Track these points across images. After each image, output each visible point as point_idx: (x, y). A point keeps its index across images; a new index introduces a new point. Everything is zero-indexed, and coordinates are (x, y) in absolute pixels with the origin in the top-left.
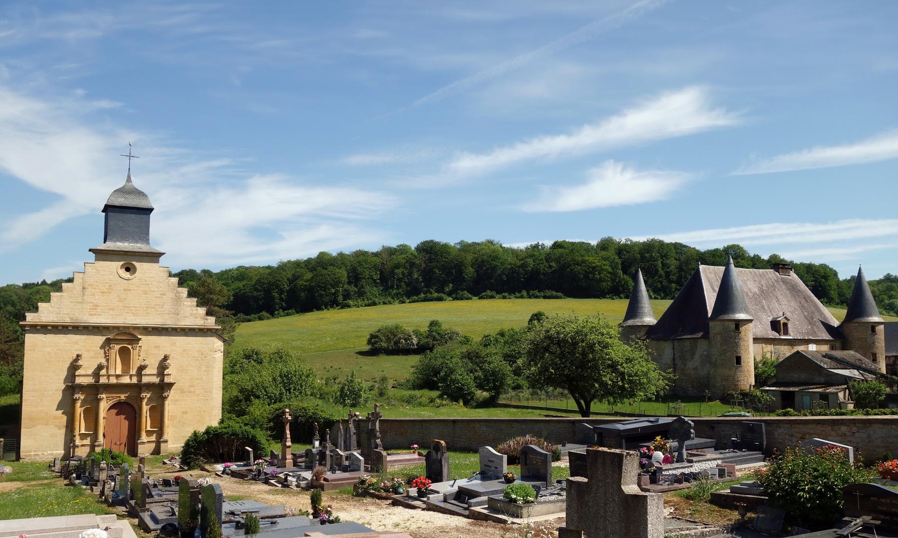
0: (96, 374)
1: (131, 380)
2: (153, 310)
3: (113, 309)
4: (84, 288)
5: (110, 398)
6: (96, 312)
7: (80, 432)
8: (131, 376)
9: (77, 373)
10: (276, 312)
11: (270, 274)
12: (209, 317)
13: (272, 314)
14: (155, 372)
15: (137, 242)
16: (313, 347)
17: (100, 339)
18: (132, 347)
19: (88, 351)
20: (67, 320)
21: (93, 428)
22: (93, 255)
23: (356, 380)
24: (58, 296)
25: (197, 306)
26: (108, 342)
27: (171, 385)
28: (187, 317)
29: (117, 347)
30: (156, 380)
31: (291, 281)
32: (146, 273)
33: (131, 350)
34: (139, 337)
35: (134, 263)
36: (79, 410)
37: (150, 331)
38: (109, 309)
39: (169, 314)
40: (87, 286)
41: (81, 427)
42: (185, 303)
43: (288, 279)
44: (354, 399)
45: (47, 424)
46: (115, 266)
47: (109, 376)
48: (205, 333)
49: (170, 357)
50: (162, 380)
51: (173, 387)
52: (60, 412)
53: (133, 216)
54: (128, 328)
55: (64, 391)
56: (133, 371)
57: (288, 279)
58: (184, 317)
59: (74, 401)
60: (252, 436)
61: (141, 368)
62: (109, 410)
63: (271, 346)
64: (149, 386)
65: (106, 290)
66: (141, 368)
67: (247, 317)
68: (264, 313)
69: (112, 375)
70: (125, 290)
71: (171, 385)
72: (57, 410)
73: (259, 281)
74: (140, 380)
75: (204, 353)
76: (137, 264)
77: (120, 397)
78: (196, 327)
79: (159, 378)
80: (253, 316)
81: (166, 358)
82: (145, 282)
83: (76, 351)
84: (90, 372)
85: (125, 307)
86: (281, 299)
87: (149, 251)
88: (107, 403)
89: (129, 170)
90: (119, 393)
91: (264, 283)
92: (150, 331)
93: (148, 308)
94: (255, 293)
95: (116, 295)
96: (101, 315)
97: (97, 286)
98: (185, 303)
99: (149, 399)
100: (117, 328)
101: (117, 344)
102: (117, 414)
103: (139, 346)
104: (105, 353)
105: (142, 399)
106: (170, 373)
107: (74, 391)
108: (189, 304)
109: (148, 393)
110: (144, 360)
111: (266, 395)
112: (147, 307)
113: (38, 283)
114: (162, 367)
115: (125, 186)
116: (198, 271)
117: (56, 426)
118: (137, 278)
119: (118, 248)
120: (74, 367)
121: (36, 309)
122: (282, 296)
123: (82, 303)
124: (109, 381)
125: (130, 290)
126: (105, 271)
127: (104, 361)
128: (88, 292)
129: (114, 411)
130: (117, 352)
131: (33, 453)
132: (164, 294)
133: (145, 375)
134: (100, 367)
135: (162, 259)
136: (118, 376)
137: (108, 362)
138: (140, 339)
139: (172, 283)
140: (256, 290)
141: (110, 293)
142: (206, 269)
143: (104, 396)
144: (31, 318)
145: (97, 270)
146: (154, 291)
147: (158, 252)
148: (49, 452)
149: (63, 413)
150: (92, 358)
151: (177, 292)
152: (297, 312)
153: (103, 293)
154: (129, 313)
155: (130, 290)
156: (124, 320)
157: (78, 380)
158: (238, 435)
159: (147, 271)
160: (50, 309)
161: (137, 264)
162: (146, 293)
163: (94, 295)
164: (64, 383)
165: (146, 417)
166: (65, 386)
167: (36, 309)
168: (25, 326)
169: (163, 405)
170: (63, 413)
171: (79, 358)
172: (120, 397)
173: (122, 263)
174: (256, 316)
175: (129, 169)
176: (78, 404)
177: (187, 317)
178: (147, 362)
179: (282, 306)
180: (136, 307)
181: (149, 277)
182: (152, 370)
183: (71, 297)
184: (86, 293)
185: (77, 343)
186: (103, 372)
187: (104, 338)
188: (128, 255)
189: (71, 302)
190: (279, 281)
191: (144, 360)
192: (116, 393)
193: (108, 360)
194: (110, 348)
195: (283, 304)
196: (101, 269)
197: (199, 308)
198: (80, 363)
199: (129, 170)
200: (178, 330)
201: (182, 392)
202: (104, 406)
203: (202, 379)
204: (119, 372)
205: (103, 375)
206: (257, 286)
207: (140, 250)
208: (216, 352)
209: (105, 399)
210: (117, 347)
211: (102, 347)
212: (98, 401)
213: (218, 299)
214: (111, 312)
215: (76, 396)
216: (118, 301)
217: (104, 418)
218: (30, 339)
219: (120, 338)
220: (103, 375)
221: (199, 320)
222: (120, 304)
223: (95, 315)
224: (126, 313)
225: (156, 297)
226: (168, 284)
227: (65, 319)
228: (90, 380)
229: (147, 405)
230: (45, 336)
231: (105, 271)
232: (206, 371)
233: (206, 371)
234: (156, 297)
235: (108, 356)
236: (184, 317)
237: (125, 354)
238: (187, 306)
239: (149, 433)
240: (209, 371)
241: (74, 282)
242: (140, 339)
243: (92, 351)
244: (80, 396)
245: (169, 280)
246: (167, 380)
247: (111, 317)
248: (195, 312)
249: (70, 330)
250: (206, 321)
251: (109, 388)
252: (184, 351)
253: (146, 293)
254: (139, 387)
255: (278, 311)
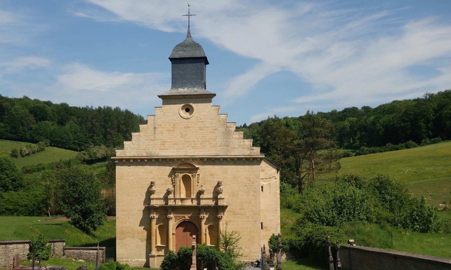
0: (166, 198)
1: (192, 203)
2: (208, 143)
3: (176, 144)
4: (155, 128)
5: (178, 218)
6: (164, 147)
7: (156, 245)
8: (192, 200)
9: (152, 197)
10: (423, 141)
11: (416, 106)
12: (255, 148)
13: (419, 142)
14: (211, 196)
15: (194, 87)
16: (444, 172)
17: (168, 169)
18: (192, 176)
19: (160, 179)
20: (143, 154)
21: (166, 243)
22: (161, 100)
23: (426, 205)
24: (137, 136)
25: (130, 140)
26: (174, 171)
27: (224, 208)
28: (236, 148)
29: (181, 175)
30: (211, 203)
31: (436, 111)
32: (201, 112)
33: (192, 178)
34: (197, 166)
35: (191, 104)
36: (155, 227)
37: (206, 162)
38: (174, 144)
39: (221, 146)
40: (157, 126)
41: (157, 241)
42: (234, 136)
43: (434, 109)
44: (424, 224)
45: (133, 237)
46: (177, 108)
47: (175, 199)
48: (251, 162)
49: (222, 184)
50: (216, 203)
51: (227, 210)
52: (142, 228)
53: (180, 63)
54: (188, 159)
55: (144, 211)
56: (194, 196)
57: (434, 109)
58: (234, 148)
59: (151, 219)
60: (216, 259)
61: (200, 193)
62: (177, 227)
63: (404, 172)
64: (206, 208)
65: (171, 129)
66: (200, 193)
67: (394, 146)
68: (411, 142)
69: (178, 199)
70: (185, 128)
71: (224, 208)
72: (140, 226)
73: (406, 112)
74: (199, 203)
75: (252, 180)
76: (194, 105)
77: (185, 217)
78: (243, 156)
79: (214, 202)
80: (400, 144)
81: (219, 184)
82: (200, 120)
83: (151, 178)
84: (162, 196)
85: (186, 142)
86: (428, 128)
87: (202, 93)
88: (175, 221)
89: (189, 27)
90: (184, 214)
91: (410, 115)
92: (206, 162)
93: (204, 141)
94: (403, 124)
95: (179, 132)
96: (168, 149)
97: (165, 125)
98: (234, 136)
99: (207, 219)
100: (178, 159)
101: (180, 173)
102: (184, 231)
103: (198, 175)
104: (172, 180)
105: (201, 219)
106: (222, 197)
107: (150, 212)
108: (237, 136)
109: (206, 214)
110: (202, 186)
111: (318, 219)
112: (203, 141)
113: (241, 126)
114: (217, 192)
115: (185, 40)
116: (360, 108)
117: (139, 239)
118: (194, 117)
119: (179, 93)
120: (150, 192)
121: (122, 147)
122: (429, 125)
123: (154, 140)
124: (175, 203)
125: (189, 127)
126: (170, 113)
127: (171, 187)
128: (158, 131)
129: (181, 229)
130: (181, 180)
131: (124, 260)
132: (216, 129)
133: (203, 199)
134: (168, 192)
135: (213, 99)
136: (182, 200)
137: (175, 188)
138: (198, 169)
139: (222, 119)
140: (404, 121)
141: (174, 131)
142: (366, 105)
143: (172, 216)
144: (119, 153)
145: (164, 112)
146: (208, 127)
147: (210, 93)
148: (136, 260)
149: (144, 229)
150: (162, 184)
151: (227, 127)
152: (443, 140)
153: (169, 131)
154: (189, 147)
155: (189, 127)
156: (185, 153)
157: (153, 203)
158: (204, 256)
159: (202, 111)
160: (132, 146)
161: (194, 105)
162: (201, 129)
163: (162, 133)
164: (144, 205)
165: (206, 234)
166: (144, 207)
167: (122, 147)
168: (115, 160)
169: (218, 225)
170: (144, 229)
171: (152, 185)
172: (185, 217)
173: (182, 105)
174: (403, 145)
175: (189, 26)
176: (154, 222)
177: (236, 148)
178: (204, 188)
179: (429, 134)
180: (194, 141)
181: (204, 115)
182: (208, 194)
183: (146, 136)
184: (157, 132)
185: (151, 172)
186: (171, 196)
187: (171, 168)
188: (187, 98)
189: (146, 140)
190: (425, 111)
191: (202, 186)
192: (182, 214)
193: (174, 186)
194: (175, 176)
195: (430, 132)
196: (167, 111)
197: (245, 140)
198: (154, 188)
199: (189, 27)
200: (228, 160)
201: (235, 214)
202: (173, 224)
203: (251, 203)
204: (183, 196)
205: (171, 199)
206: (404, 118)
207: (196, 93)
208: (271, 178)
209: (174, 218)
210: (181, 175)
211: (170, 176)
212: (168, 219)
213: (321, 131)
214: (176, 147)
215: (152, 215)
216: (181, 137)
217: (173, 234)
218: (120, 170)
219: (182, 168)
220: (171, 199)
221: (246, 151)
222: (182, 139)
223: (164, 149)
224: (187, 146)
225: (210, 132)
226: (219, 120)
227: (142, 154)
228: (161, 203)
229: (205, 224)
230: (129, 167)
231: (170, 113)
232: (254, 196)
233: (254, 196)
234: (210, 132)
235: (174, 182)
236: (234, 148)
237: (187, 180)
238: (236, 139)
239: (159, 249)
240: (256, 196)
241: (148, 124)
242: (198, 169)
243: (162, 179)
244: (155, 216)
245: (220, 116)
246: (221, 203)
247: (175, 150)
248: (242, 143)
249: (146, 162)
250: (252, 151)
251: (175, 209)
252: (234, 178)
253: (201, 129)
254: (198, 209)
255: (425, 139)
